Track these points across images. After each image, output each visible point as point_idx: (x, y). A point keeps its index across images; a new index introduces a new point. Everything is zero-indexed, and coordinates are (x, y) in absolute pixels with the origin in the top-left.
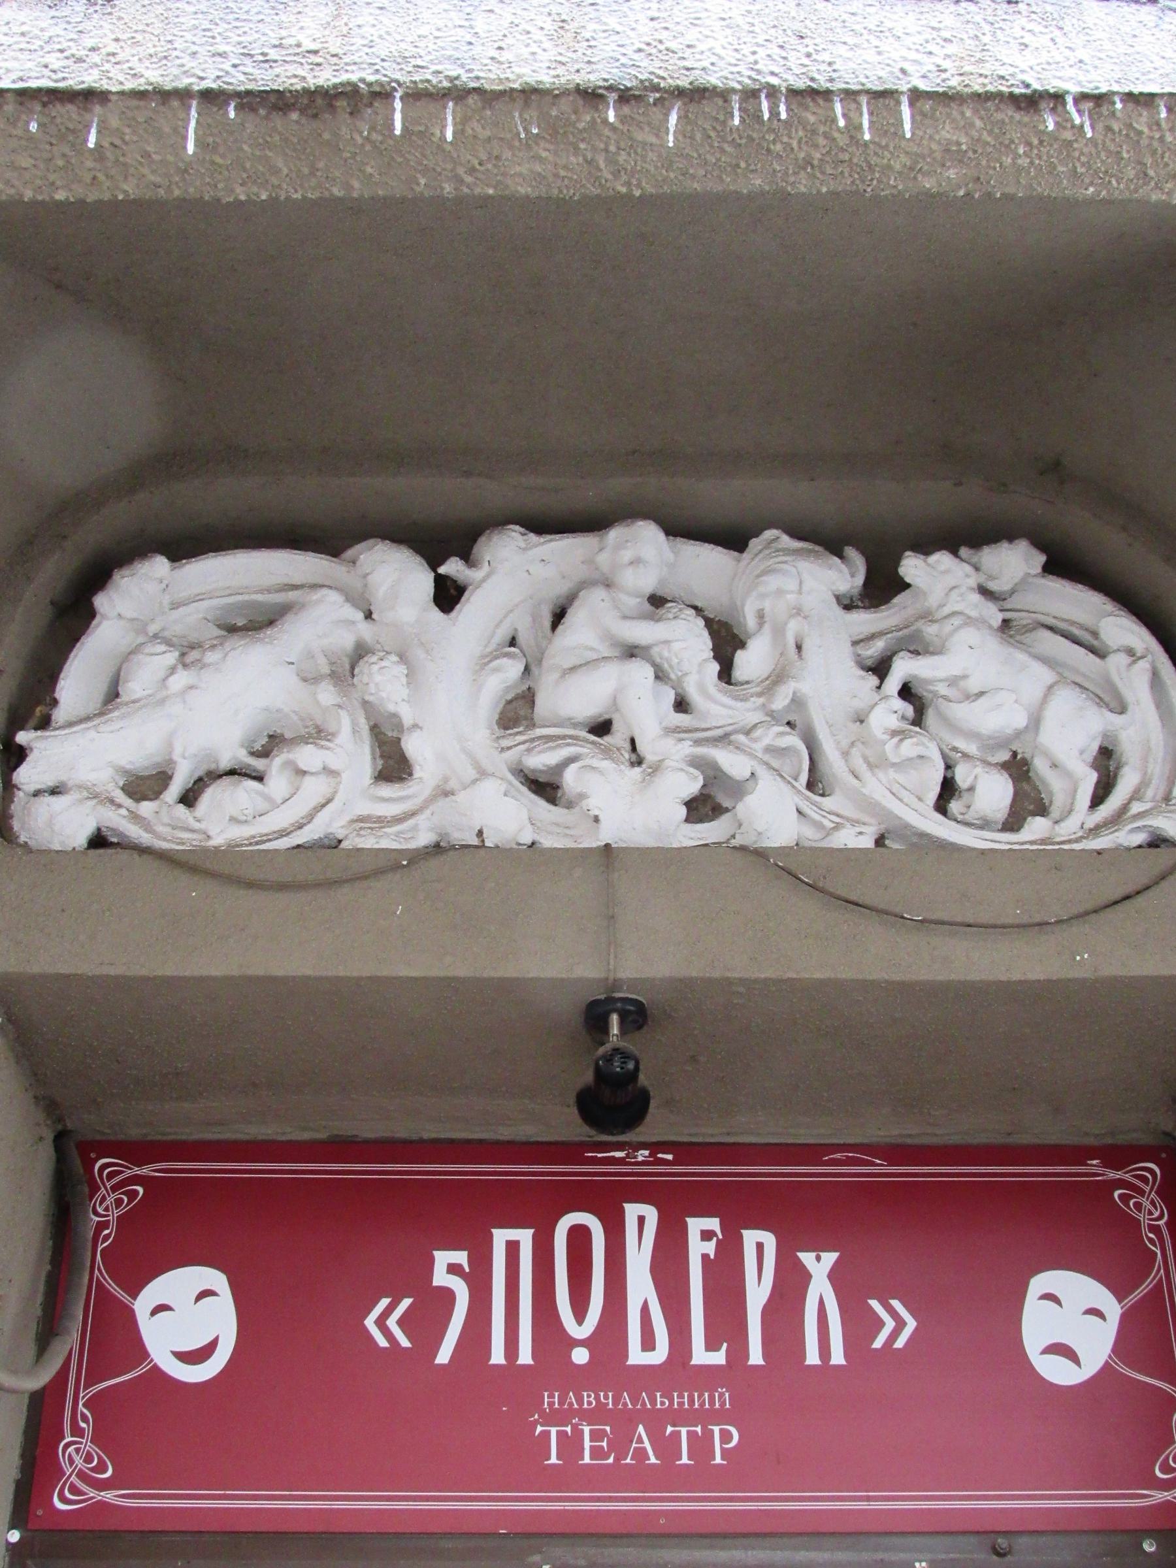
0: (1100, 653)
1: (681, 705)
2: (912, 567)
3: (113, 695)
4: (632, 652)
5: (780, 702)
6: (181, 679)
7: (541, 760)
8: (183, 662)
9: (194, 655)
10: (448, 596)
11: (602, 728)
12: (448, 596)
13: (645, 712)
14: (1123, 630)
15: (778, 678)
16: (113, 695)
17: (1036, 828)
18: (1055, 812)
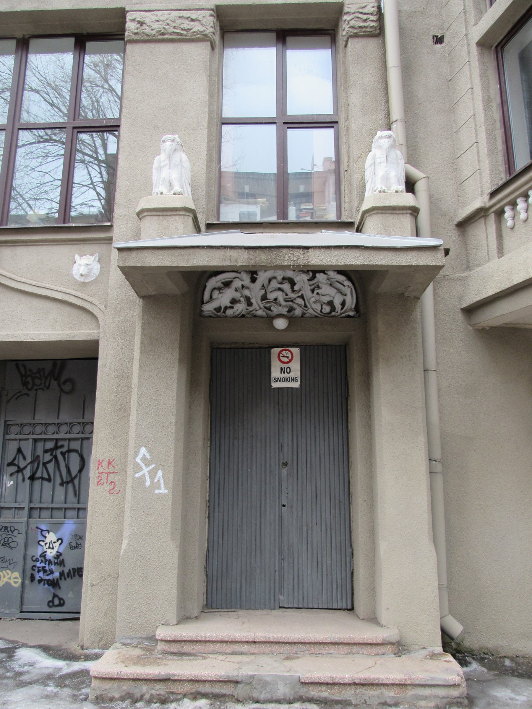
0: (344, 286)
1: (287, 295)
2: (317, 275)
3: (211, 297)
4: (280, 289)
5: (300, 294)
6: (220, 295)
7: (268, 305)
8: (220, 293)
9: (221, 291)
10: (253, 280)
11: (276, 299)
12: (253, 280)
13: (281, 299)
14: (347, 283)
15: (300, 290)
16: (211, 297)
17: (333, 313)
18: (336, 311)
